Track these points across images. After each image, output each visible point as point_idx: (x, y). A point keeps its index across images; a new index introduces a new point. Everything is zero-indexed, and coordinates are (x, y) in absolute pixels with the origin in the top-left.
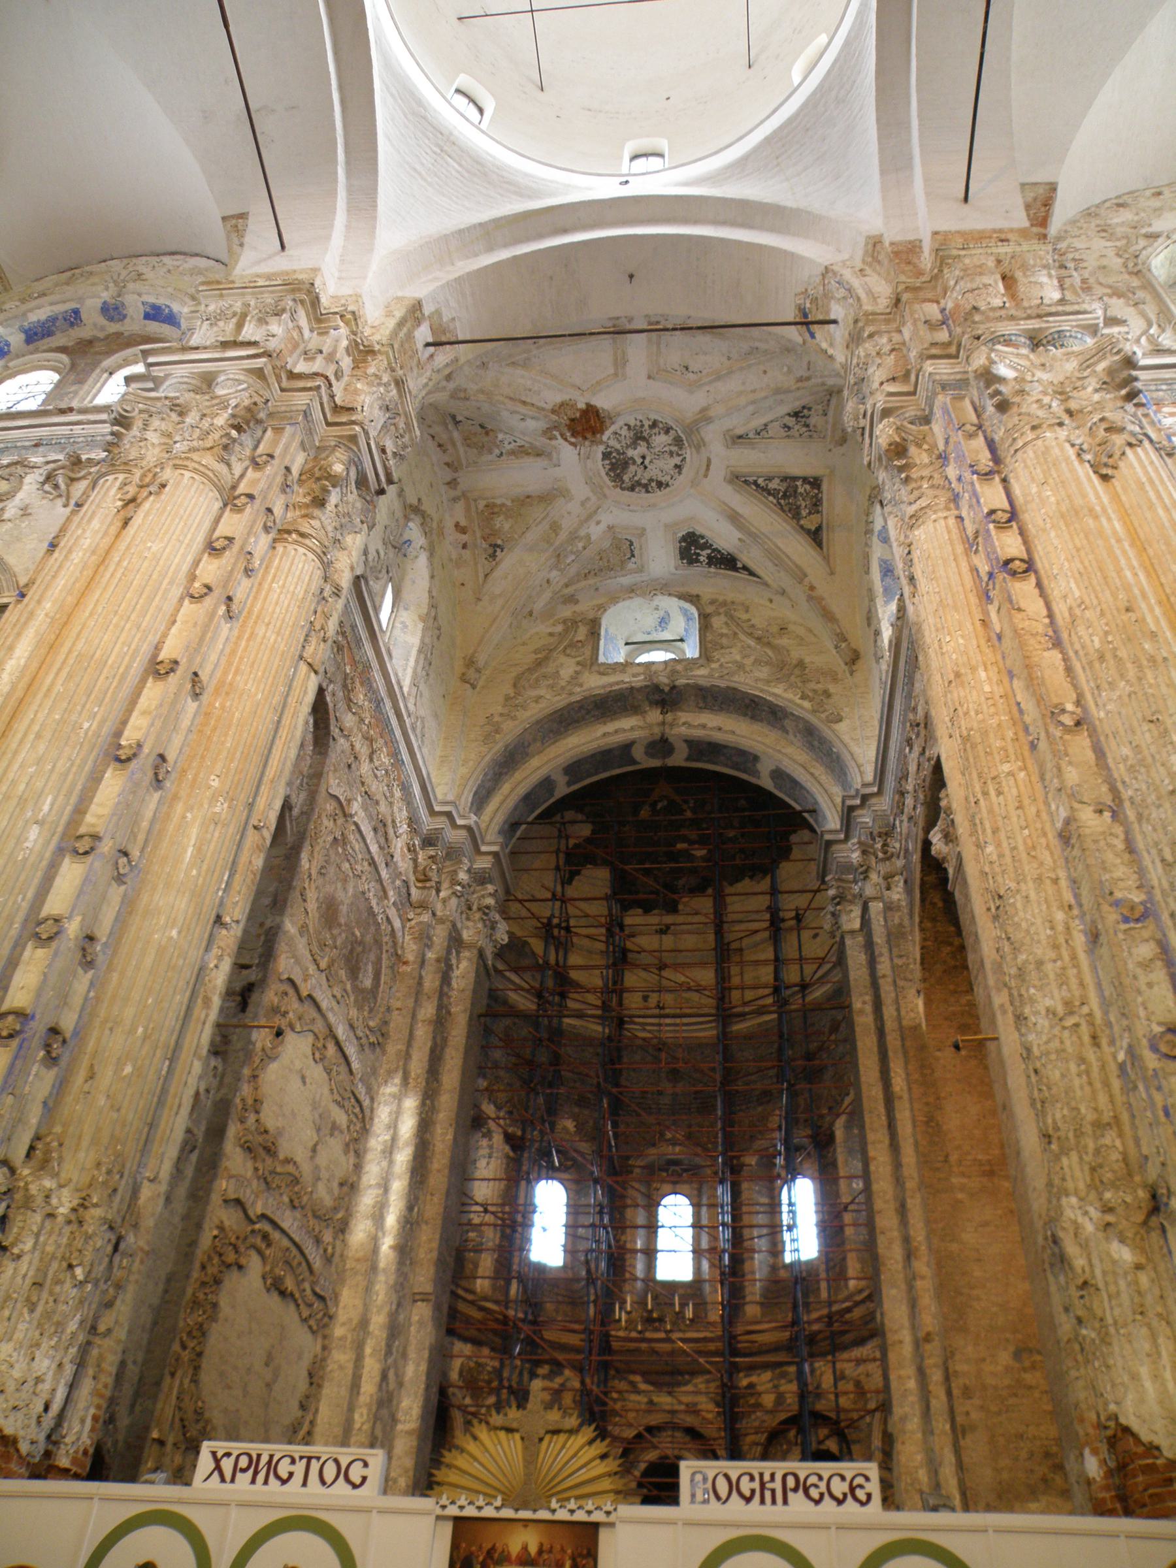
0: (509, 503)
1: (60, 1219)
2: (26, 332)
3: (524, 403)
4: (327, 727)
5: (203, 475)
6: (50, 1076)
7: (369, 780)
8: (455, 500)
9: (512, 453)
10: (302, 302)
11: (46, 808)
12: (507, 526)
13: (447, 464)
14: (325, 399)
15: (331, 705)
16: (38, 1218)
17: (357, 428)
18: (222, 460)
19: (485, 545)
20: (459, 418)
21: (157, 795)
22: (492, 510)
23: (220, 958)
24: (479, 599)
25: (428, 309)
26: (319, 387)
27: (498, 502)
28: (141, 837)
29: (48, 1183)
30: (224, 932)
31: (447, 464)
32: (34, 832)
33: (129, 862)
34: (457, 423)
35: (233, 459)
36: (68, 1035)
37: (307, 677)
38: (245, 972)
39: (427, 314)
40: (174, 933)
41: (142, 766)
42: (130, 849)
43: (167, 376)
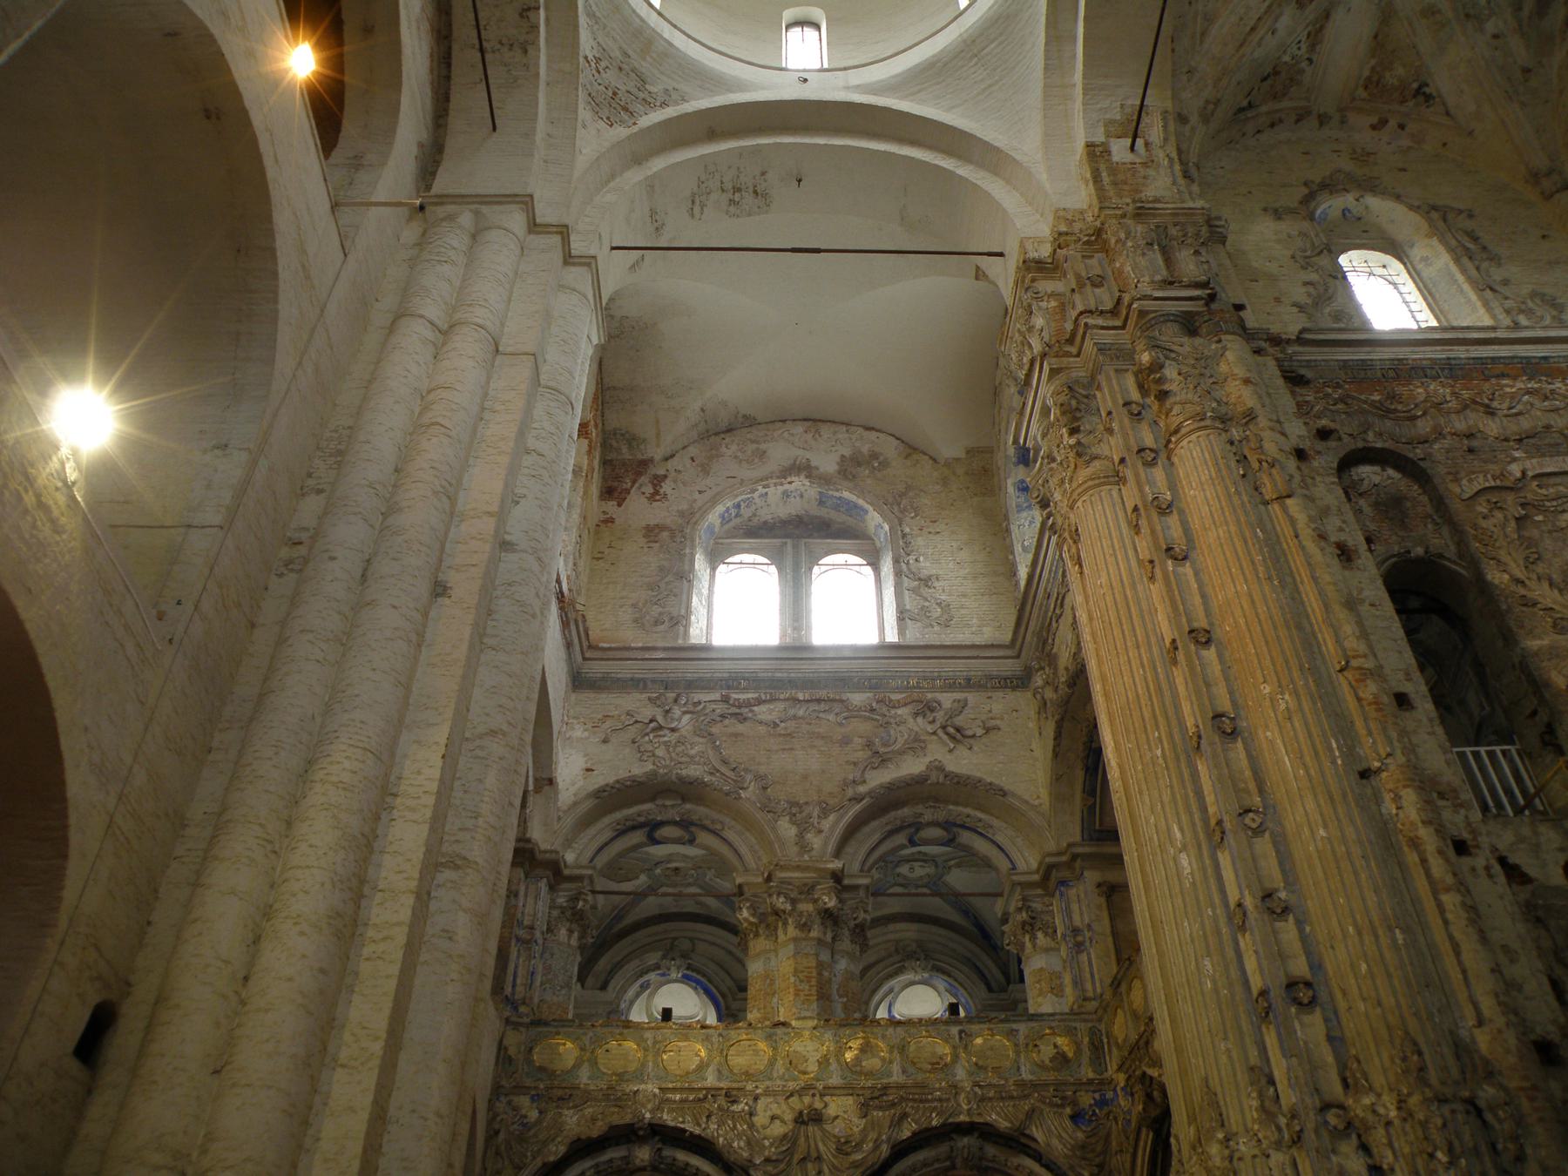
0: (1373, 62)
1: (1396, 1122)
2: (1019, 462)
3: (1253, 29)
4: (1407, 459)
5: (1086, 490)
6: (1315, 1019)
7: (1513, 428)
8: (1343, 121)
9: (1313, 47)
10: (1033, 280)
11: (1178, 835)
12: (1400, 71)
13: (1298, 121)
14: (1100, 322)
15: (1389, 445)
16: (1381, 1131)
17: (1135, 306)
18: (1088, 463)
19: (1411, 104)
20: (1245, 103)
21: (1240, 744)
22: (1374, 84)
23: (1397, 798)
24: (1471, 133)
25: (1100, 138)
26: (1086, 324)
27: (1366, 73)
28: (1252, 786)
29: (1367, 1101)
30: (1384, 775)
31: (1298, 121)
32: (1184, 860)
33: (1257, 812)
34: (1250, 106)
35: (1095, 450)
36: (1308, 976)
37: (1285, 510)
38: (1537, 718)
39: (1102, 139)
40: (1322, 832)
41: (1210, 737)
42: (1247, 803)
43: (1035, 438)
